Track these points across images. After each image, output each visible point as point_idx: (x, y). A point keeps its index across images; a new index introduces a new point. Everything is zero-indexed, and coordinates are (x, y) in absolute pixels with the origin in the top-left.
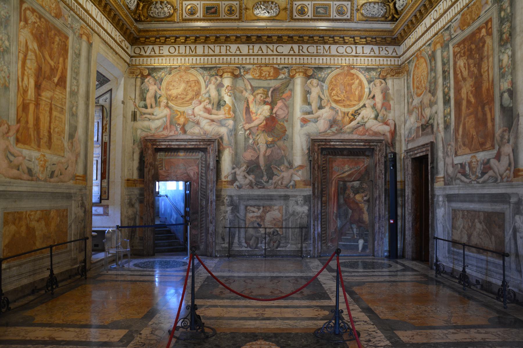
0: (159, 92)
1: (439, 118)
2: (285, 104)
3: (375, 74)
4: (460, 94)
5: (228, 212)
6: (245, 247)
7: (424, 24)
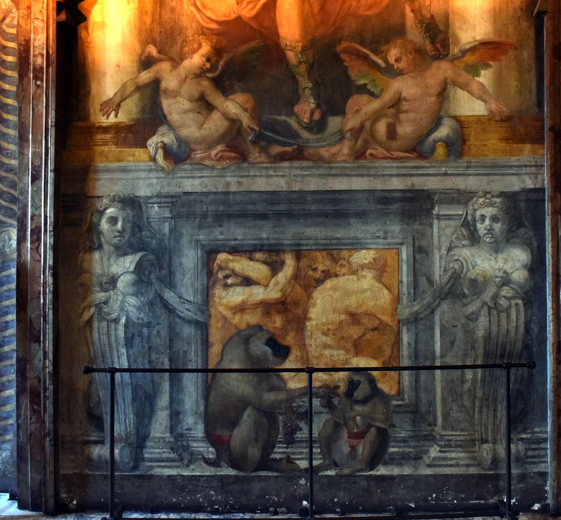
5: (120, 285)
6: (208, 462)
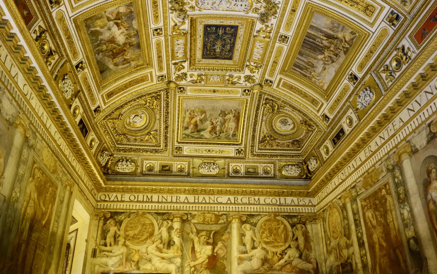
0: (118, 232)
1: (357, 258)
2: (224, 245)
3: (296, 220)
4: (372, 239)
7: (333, 182)
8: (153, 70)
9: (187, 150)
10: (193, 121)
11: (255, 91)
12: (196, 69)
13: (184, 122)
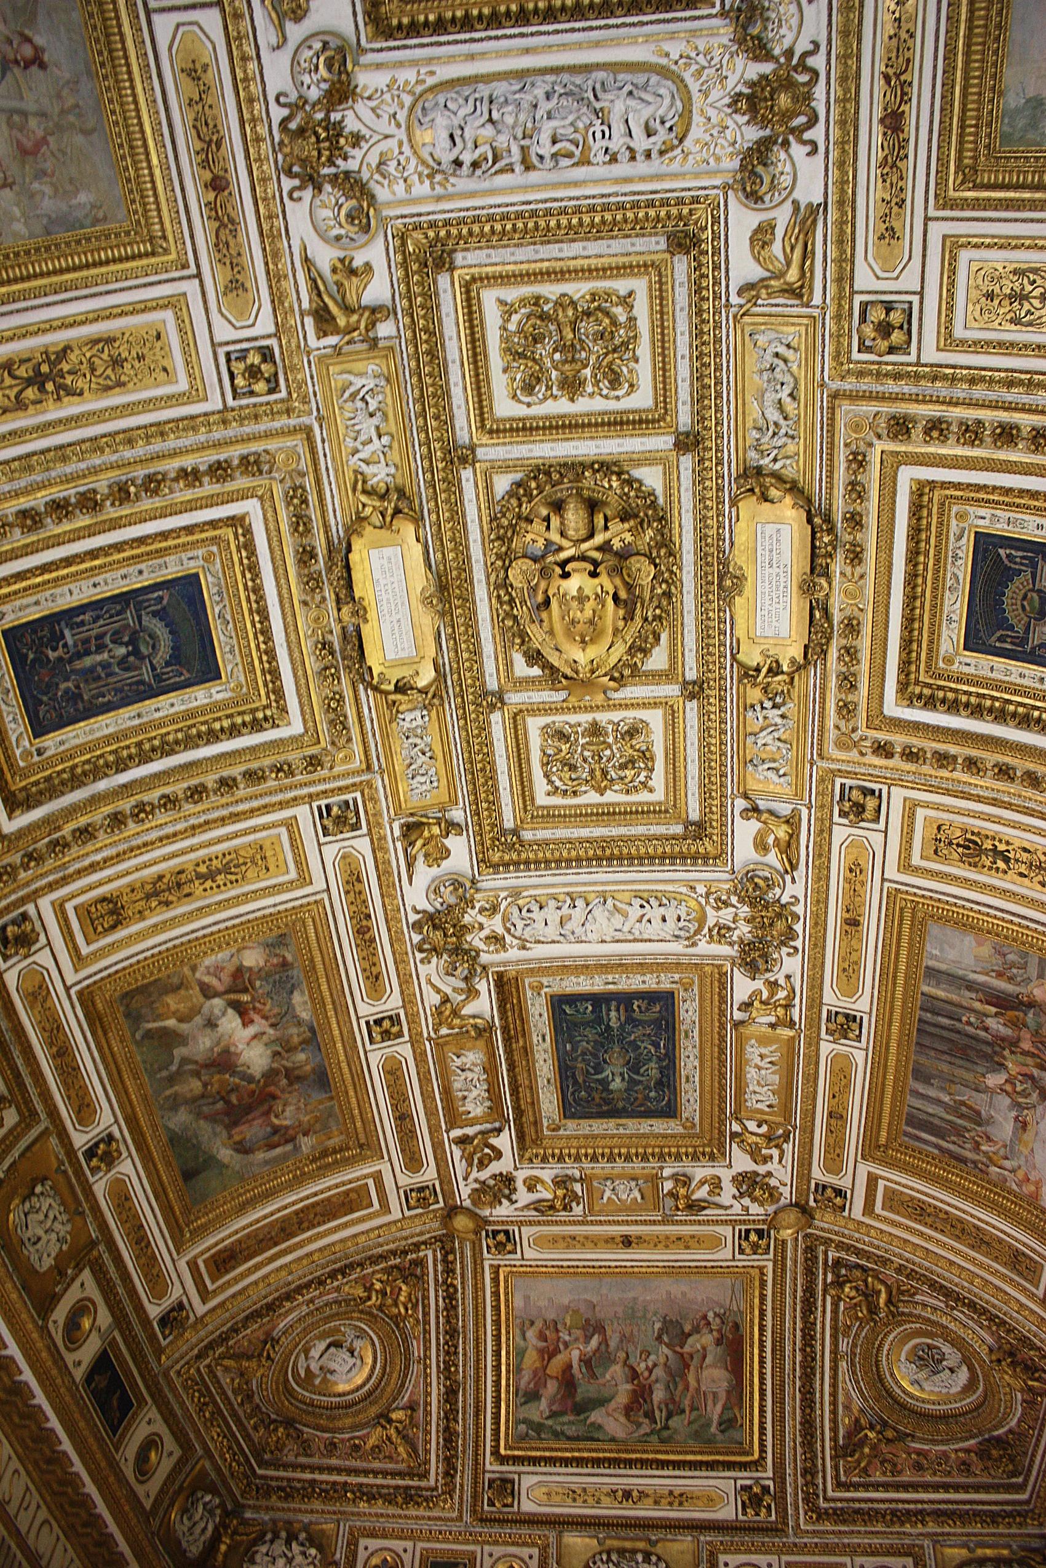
8: (384, 1167)
9: (537, 1490)
10: (556, 1364)
11: (787, 1234)
12: (544, 1159)
13: (519, 1370)
